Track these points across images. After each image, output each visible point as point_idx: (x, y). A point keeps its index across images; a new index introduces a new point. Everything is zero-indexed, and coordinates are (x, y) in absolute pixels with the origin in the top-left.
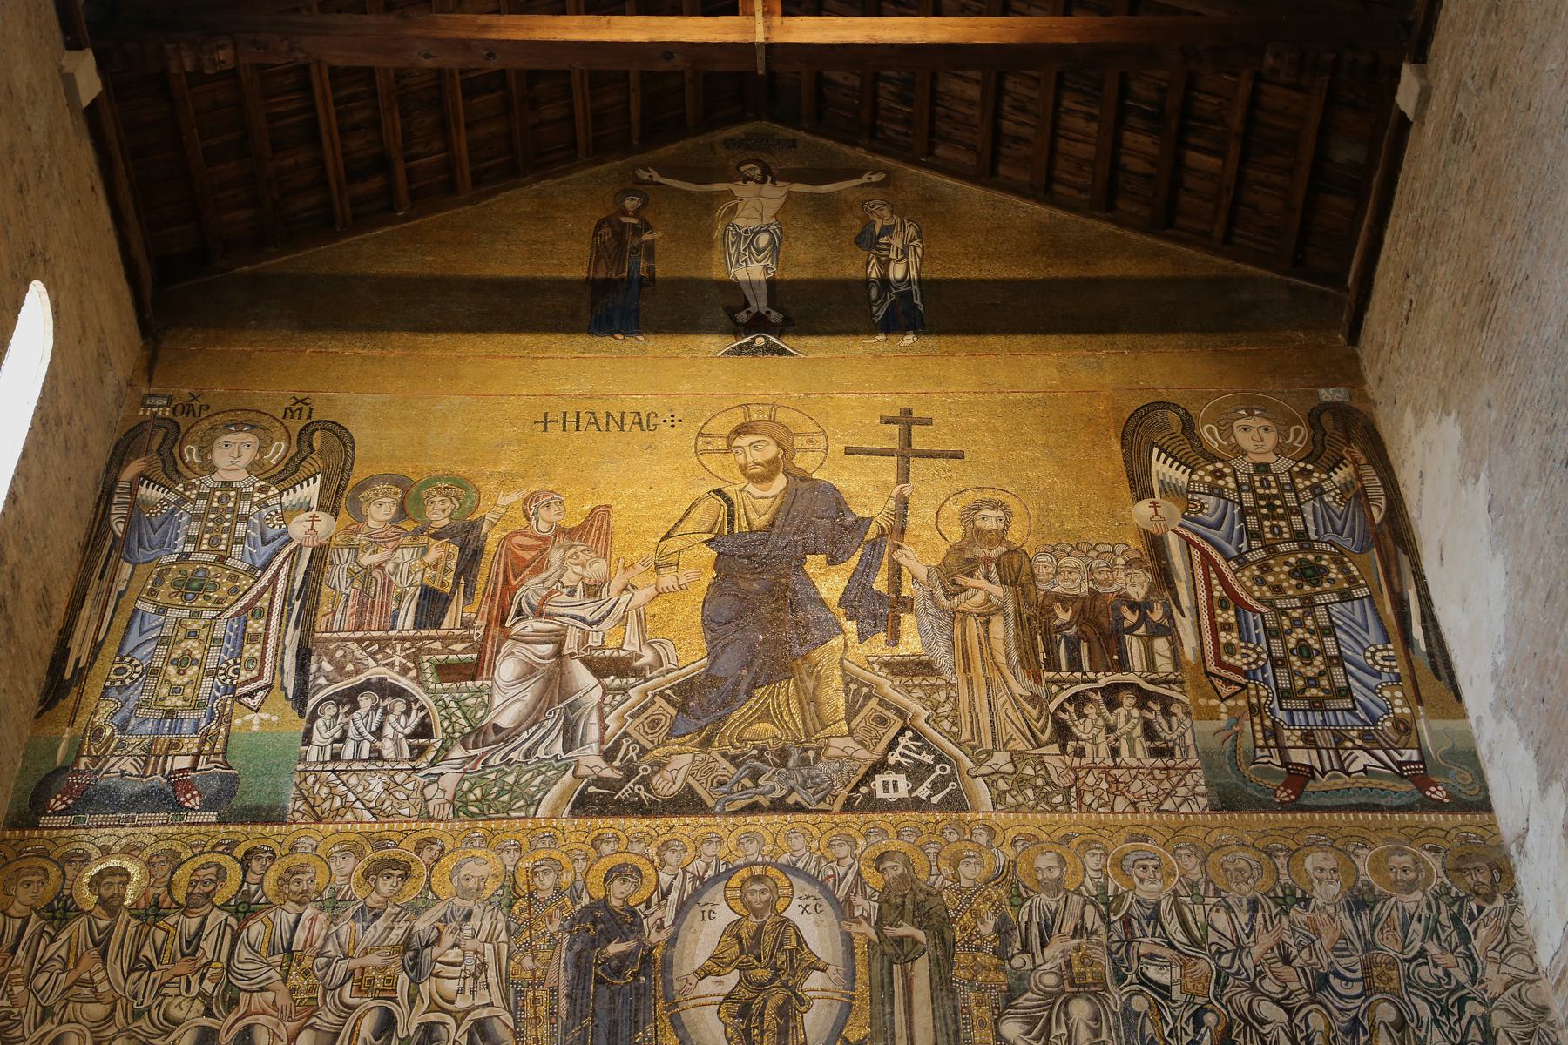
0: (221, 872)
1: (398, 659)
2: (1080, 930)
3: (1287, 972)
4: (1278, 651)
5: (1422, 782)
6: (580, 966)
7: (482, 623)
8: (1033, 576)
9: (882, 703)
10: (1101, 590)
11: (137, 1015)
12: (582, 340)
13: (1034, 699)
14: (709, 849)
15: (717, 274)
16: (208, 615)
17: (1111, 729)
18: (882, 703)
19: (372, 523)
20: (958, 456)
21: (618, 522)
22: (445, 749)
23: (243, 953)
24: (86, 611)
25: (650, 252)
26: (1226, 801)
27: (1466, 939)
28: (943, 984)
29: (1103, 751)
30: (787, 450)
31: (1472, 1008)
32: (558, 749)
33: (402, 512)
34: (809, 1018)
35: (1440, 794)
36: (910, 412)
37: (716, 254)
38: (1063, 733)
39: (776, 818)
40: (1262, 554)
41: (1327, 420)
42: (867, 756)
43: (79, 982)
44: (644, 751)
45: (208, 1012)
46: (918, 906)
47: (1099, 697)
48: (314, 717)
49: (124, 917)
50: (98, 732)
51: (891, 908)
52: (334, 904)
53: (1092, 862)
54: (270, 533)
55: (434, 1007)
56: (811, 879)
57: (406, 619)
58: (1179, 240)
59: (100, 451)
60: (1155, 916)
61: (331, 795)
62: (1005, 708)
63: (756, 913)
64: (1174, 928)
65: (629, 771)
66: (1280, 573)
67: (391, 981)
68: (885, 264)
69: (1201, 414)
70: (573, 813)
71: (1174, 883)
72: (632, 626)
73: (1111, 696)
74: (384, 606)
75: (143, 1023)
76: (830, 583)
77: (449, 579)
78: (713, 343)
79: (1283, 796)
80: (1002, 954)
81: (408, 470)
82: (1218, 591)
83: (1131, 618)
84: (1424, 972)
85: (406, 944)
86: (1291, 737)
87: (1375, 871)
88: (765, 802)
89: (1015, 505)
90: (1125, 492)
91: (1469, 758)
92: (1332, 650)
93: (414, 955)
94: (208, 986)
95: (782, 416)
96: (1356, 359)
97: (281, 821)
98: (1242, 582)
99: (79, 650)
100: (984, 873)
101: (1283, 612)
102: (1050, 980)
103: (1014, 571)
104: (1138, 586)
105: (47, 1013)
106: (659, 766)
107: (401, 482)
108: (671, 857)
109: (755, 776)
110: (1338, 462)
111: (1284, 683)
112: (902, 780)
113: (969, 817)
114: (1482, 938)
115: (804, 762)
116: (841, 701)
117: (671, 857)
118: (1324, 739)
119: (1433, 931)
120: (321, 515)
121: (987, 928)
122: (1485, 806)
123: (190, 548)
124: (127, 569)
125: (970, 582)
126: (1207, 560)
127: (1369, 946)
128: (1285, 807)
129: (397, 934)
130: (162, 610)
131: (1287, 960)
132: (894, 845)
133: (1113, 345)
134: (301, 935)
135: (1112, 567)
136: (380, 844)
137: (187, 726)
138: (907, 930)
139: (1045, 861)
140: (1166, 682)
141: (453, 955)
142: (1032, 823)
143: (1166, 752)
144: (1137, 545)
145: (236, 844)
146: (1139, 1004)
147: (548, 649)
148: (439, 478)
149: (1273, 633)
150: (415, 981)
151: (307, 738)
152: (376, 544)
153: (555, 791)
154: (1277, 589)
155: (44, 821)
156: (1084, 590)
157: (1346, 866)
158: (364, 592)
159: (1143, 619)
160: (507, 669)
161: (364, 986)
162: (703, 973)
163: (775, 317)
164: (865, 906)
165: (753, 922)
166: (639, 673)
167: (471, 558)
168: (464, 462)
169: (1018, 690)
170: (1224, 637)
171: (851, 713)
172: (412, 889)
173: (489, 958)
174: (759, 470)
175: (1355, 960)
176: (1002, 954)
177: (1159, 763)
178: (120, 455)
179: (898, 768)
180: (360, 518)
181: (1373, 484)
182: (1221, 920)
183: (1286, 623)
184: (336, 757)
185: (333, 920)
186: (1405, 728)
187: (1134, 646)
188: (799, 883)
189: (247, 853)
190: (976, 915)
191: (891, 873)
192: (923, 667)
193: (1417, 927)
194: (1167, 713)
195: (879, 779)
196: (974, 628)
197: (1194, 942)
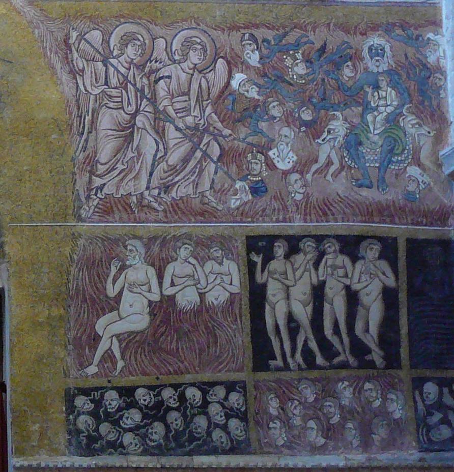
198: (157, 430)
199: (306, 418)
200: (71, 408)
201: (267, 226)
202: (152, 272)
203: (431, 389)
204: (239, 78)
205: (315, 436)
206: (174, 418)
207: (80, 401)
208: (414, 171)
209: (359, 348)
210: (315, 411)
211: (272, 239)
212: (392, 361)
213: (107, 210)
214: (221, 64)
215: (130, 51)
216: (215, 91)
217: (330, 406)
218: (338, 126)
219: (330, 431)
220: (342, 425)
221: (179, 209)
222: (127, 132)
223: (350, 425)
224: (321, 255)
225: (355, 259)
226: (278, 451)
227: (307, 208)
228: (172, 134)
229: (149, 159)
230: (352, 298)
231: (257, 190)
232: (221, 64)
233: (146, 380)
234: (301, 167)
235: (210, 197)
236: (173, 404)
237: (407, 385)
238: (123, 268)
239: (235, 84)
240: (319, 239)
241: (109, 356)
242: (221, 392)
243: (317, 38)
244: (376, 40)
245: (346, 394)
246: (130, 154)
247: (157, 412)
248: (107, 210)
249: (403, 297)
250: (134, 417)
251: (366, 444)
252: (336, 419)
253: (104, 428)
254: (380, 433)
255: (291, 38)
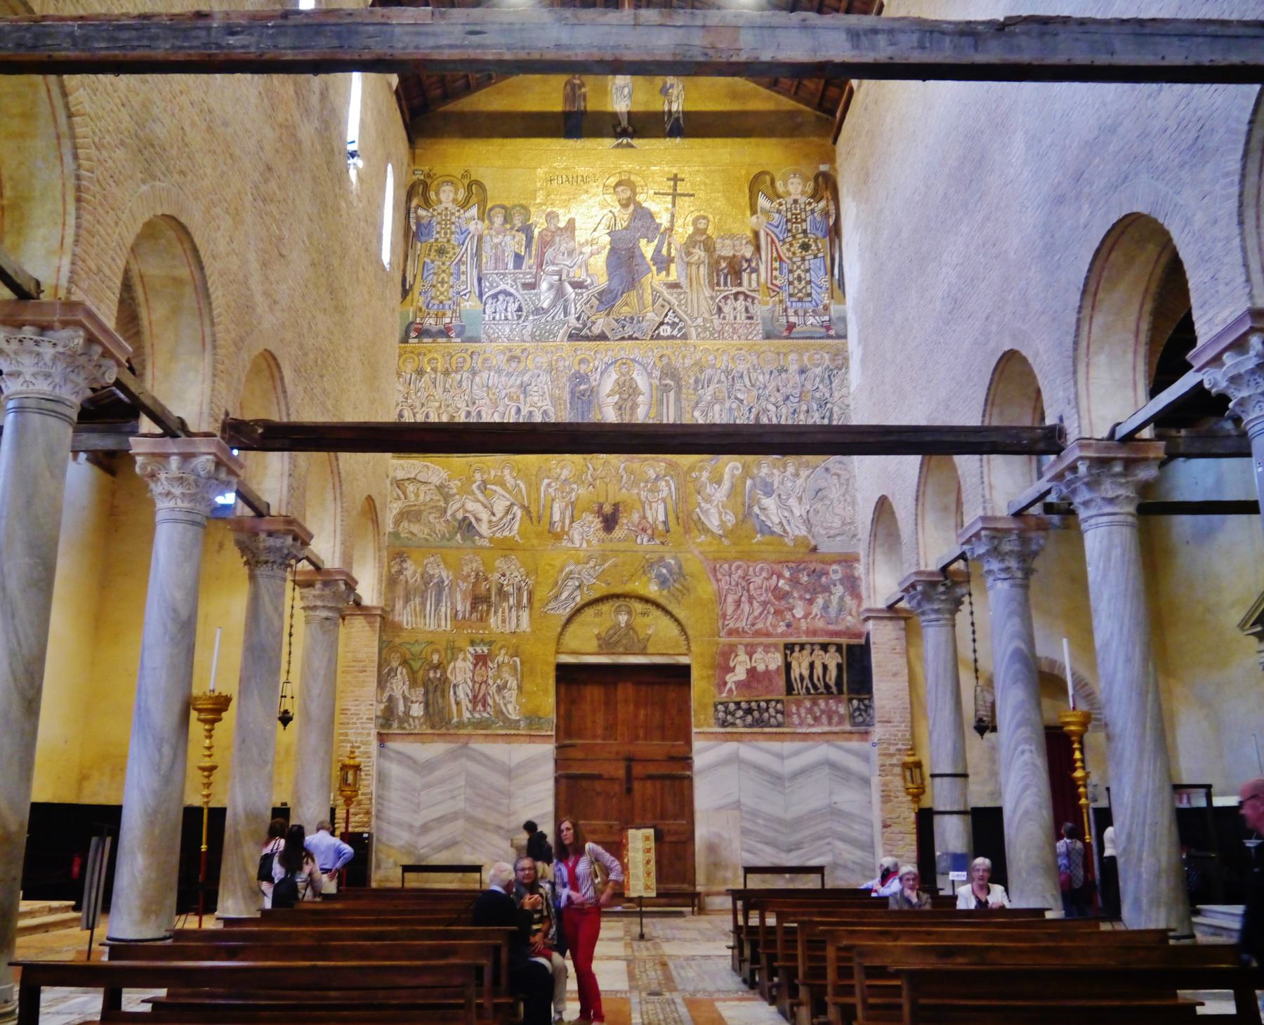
0: (465, 359)
1: (509, 281)
2: (719, 382)
3: (778, 395)
4: (791, 279)
5: (828, 328)
6: (572, 393)
7: (535, 267)
8: (715, 248)
9: (664, 300)
10: (737, 254)
11: (448, 406)
12: (563, 141)
13: (712, 298)
14: (609, 353)
15: (609, 109)
16: (448, 263)
17: (735, 309)
18: (664, 300)
19: (496, 225)
20: (692, 195)
21: (577, 225)
22: (527, 316)
23: (475, 387)
24: (409, 262)
25: (585, 99)
26: (768, 336)
27: (831, 383)
28: (678, 400)
29: (732, 318)
30: (635, 194)
31: (829, 406)
32: (562, 316)
33: (506, 221)
34: (639, 410)
35: (832, 332)
36: (676, 175)
37: (609, 98)
38: (720, 310)
39: (630, 342)
40: (790, 239)
41: (820, 179)
42: (659, 320)
43: (429, 395)
44: (589, 318)
45: (467, 406)
46: (672, 373)
47: (732, 297)
48: (485, 304)
49: (439, 374)
50: (420, 310)
51: (664, 374)
52: (499, 371)
53: (725, 358)
54: (463, 230)
55: (531, 406)
56: (640, 364)
57: (511, 266)
58: (779, 92)
59: (404, 198)
60: (742, 377)
61: (494, 333)
62: (703, 303)
63: (624, 375)
64: (747, 380)
65: (585, 325)
66: (796, 245)
67: (518, 397)
68: (670, 103)
69: (778, 176)
70: (568, 340)
71: (748, 365)
72: (584, 269)
73: (736, 295)
74: (503, 260)
75: (450, 408)
76: (648, 249)
77: (523, 249)
78: (609, 142)
79: (785, 334)
80: (695, 390)
81: (506, 203)
82: (775, 255)
83: (745, 265)
84: (817, 395)
85: (522, 385)
86: (791, 312)
87: (809, 360)
88: (626, 336)
89: (711, 217)
90: (748, 213)
91: (843, 319)
92: (808, 279)
93: (524, 388)
94: (466, 397)
95: (633, 178)
96: (834, 151)
97: (480, 342)
98: (783, 250)
99: (409, 279)
100: (692, 362)
101: (794, 263)
102: (709, 398)
103: (709, 247)
104: (748, 252)
105: (423, 405)
106: (594, 323)
107: (503, 207)
108: (598, 356)
109: (623, 327)
110: (822, 199)
111: (791, 292)
112: (669, 328)
113: (688, 341)
114: (836, 382)
115: (639, 322)
116: (650, 298)
117: (598, 356)
118: (801, 312)
119: (822, 381)
120: (479, 222)
121: (692, 381)
122: (844, 337)
123: (438, 236)
124: (419, 244)
125: (694, 251)
126: (773, 242)
127: (803, 386)
128: (787, 338)
129: (518, 382)
130: (433, 262)
131: (778, 391)
132: (665, 352)
133: (750, 143)
134: (491, 381)
135: (741, 244)
136: (510, 351)
137: (447, 307)
138: (668, 381)
139: (711, 357)
140: (754, 291)
141: (535, 389)
142: (708, 344)
143: (750, 318)
144: (749, 234)
145: (467, 350)
146: (734, 406)
147: (556, 278)
148: (516, 206)
149: (791, 271)
150: (525, 397)
151: (484, 313)
152: (498, 233)
153: (562, 331)
154: (794, 253)
155: (410, 341)
156: (731, 254)
157: (800, 359)
158: (496, 254)
159: (749, 266)
160: (544, 286)
161: (511, 399)
162: (609, 396)
163: (630, 129)
164: (657, 373)
165: (623, 378)
166: (586, 287)
167: (529, 239)
168: (525, 199)
169: (707, 294)
170: (775, 273)
171: (654, 303)
172: (522, 366)
173: (546, 390)
174: (624, 202)
175: (798, 391)
176: (695, 390)
177: (749, 321)
178: (410, 196)
179: (668, 323)
180: (492, 223)
181: (832, 208)
182: (761, 378)
183: (795, 267)
184: (494, 319)
185: (499, 377)
186: (826, 308)
187: (745, 276)
188: (636, 365)
189: (472, 353)
190: (689, 376)
191: (664, 362)
192: (675, 286)
193: (818, 379)
194: (753, 303)
195: (662, 328)
196: (694, 267)
197: (752, 385)
198: (749, 719)
199: (806, 714)
200: (716, 710)
201: (793, 640)
202: (747, 658)
203: (855, 702)
204: (781, 582)
205: (810, 721)
206: (756, 714)
207: (721, 707)
208: (849, 618)
209: (827, 686)
210: (810, 711)
211: (794, 645)
212: (840, 692)
213: (730, 633)
214: (775, 577)
215: (740, 572)
216: (772, 587)
217: (816, 709)
218: (820, 601)
219: (816, 719)
220: (820, 717)
221: (758, 633)
222: (738, 603)
223: (824, 716)
224: (813, 651)
225: (826, 651)
226: (795, 726)
227: (807, 633)
228: (755, 604)
229: (746, 614)
230: (825, 667)
231: (788, 626)
232: (775, 577)
233: (746, 699)
234: (805, 617)
235: (770, 629)
236: (755, 708)
237: (846, 701)
238: (736, 656)
239: (780, 584)
240: (812, 644)
241: (730, 690)
242: (773, 704)
243: (812, 567)
244: (835, 567)
245: (822, 703)
246: (739, 612)
247: (749, 711)
248: (730, 633)
249: (845, 666)
250: (740, 713)
251: (830, 723)
252: (818, 714)
253: (729, 717)
254: (835, 719)
255: (802, 566)
